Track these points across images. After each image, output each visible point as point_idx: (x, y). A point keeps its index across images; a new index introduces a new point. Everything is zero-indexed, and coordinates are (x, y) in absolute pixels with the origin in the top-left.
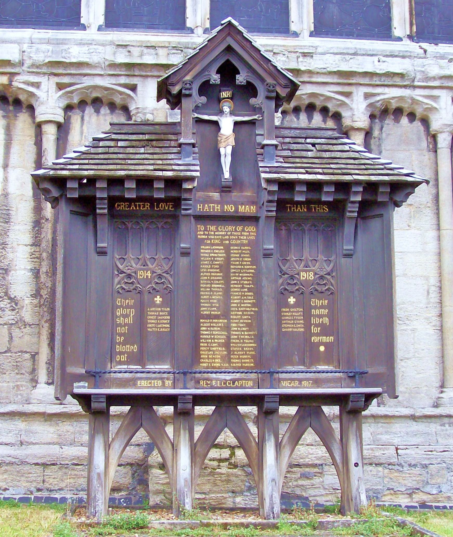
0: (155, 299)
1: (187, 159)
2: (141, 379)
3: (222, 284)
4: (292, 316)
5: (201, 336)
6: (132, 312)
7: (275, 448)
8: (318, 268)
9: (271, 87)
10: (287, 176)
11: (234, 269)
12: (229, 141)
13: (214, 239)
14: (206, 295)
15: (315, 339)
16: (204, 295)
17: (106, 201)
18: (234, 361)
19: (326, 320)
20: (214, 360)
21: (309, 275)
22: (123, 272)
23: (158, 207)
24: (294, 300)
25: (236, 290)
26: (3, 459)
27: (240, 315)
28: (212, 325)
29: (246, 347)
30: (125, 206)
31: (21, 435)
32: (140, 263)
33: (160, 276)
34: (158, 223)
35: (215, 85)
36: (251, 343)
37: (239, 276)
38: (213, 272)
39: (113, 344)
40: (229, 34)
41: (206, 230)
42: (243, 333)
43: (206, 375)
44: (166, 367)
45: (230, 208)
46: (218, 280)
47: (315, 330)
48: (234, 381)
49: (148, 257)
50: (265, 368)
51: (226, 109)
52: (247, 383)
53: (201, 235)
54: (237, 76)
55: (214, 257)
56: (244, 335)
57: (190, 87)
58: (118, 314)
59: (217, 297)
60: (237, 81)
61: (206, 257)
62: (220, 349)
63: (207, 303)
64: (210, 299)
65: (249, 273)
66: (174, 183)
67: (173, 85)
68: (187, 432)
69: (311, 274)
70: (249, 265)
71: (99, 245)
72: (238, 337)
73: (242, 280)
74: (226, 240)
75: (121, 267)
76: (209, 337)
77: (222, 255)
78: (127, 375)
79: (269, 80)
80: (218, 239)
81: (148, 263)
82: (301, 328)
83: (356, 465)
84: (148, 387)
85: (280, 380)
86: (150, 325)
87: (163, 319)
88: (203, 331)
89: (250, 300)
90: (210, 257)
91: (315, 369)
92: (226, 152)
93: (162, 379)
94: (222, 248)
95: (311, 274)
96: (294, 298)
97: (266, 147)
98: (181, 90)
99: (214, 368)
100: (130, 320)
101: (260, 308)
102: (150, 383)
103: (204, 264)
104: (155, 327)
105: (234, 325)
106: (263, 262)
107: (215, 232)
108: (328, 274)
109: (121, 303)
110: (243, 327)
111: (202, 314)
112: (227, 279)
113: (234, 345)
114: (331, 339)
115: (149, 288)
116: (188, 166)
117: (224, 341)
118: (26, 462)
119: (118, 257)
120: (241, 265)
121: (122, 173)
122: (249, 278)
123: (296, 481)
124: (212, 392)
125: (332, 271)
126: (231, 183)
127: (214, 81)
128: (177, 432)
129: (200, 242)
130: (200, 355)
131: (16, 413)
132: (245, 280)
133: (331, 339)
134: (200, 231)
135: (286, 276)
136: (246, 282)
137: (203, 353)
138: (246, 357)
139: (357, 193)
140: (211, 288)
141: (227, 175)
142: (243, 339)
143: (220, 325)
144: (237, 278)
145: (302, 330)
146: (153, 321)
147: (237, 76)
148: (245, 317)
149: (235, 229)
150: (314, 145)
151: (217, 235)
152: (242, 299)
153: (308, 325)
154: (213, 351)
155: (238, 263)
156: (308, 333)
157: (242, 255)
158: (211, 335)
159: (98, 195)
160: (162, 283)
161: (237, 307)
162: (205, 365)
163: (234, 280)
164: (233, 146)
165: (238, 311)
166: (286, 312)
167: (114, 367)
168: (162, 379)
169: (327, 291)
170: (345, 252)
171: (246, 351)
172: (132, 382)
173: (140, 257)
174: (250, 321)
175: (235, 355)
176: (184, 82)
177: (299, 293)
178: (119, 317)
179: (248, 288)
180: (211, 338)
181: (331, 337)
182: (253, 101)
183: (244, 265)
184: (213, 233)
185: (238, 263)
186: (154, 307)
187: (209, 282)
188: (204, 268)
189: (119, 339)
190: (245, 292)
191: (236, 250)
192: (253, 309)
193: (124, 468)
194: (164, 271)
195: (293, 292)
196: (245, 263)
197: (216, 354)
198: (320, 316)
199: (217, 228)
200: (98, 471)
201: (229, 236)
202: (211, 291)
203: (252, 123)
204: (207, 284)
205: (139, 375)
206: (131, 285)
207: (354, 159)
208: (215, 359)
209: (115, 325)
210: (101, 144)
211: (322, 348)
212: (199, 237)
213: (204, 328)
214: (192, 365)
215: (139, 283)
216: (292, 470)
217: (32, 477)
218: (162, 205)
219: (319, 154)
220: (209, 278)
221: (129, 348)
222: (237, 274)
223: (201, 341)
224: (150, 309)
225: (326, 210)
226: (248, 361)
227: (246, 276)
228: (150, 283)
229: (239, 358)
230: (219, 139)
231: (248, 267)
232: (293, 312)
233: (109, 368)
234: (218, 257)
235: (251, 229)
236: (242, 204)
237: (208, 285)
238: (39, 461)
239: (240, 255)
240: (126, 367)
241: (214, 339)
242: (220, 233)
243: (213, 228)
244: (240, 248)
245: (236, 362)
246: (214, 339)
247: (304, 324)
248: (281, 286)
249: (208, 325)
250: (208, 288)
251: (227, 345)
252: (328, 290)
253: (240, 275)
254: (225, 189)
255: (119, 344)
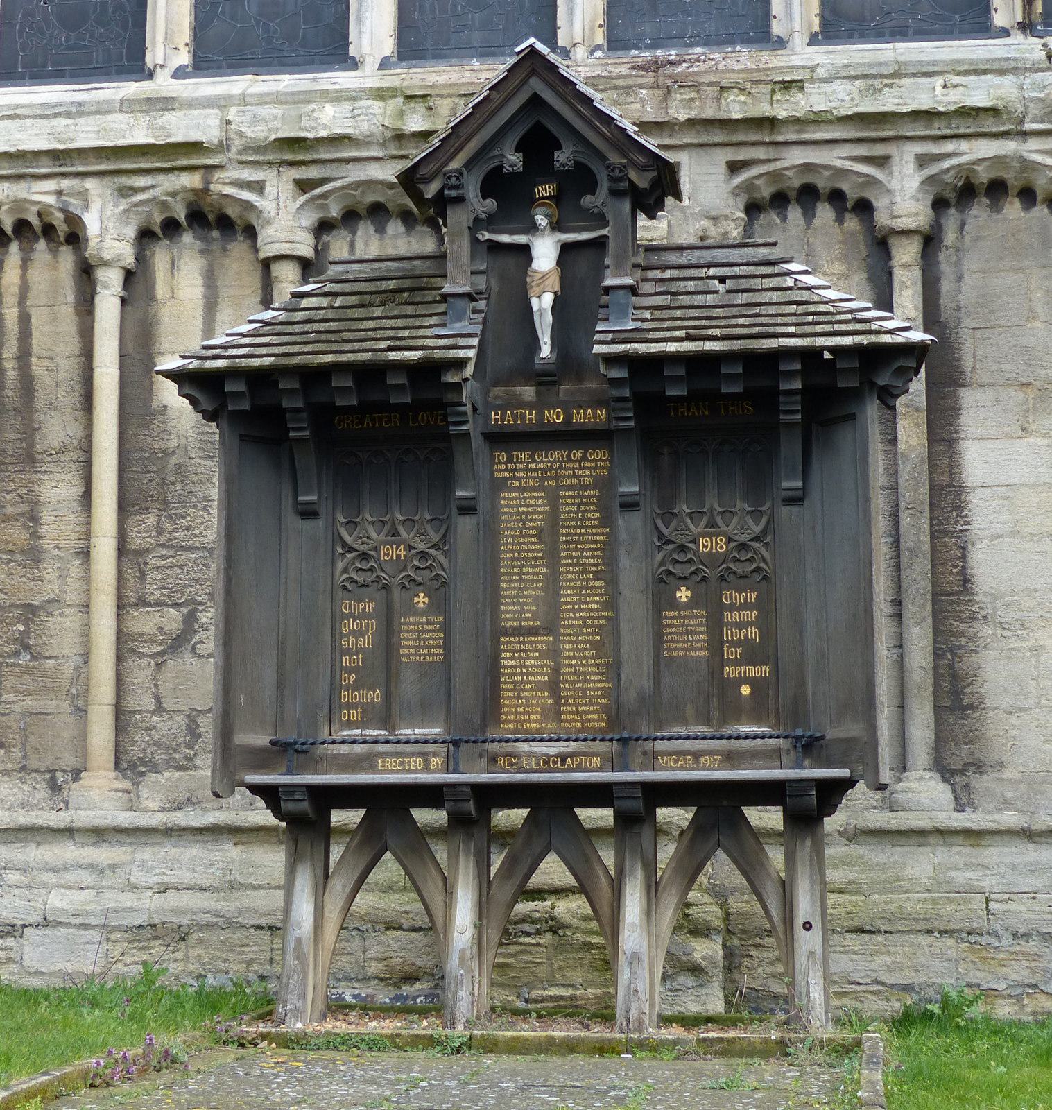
0: (416, 600)
1: (457, 325)
2: (384, 755)
3: (542, 565)
4: (684, 625)
5: (502, 670)
6: (372, 626)
7: (644, 892)
8: (736, 528)
9: (617, 170)
10: (641, 348)
11: (567, 535)
12: (547, 283)
13: (527, 478)
14: (510, 589)
15: (730, 672)
16: (508, 589)
17: (304, 415)
18: (567, 717)
19: (754, 633)
20: (527, 717)
21: (717, 544)
22: (351, 550)
23: (415, 420)
24: (689, 593)
25: (570, 576)
26: (194, 917)
27: (579, 626)
28: (523, 647)
29: (590, 689)
30: (352, 421)
31: (231, 870)
32: (385, 531)
33: (423, 555)
34: (360, 454)
35: (513, 175)
36: (601, 681)
37: (576, 549)
38: (524, 543)
39: (334, 689)
40: (533, 73)
41: (510, 460)
42: (584, 662)
43: (509, 747)
44: (434, 731)
45: (555, 417)
46: (536, 559)
47: (730, 653)
48: (563, 758)
49: (400, 518)
50: (623, 730)
51: (542, 221)
52: (590, 760)
53: (500, 471)
54: (557, 153)
55: (527, 513)
56: (587, 665)
57: (457, 183)
58: (345, 630)
59: (534, 591)
60: (557, 164)
61: (512, 514)
62: (539, 693)
63: (514, 604)
64: (518, 596)
65: (596, 542)
66: (429, 372)
67: (427, 180)
68: (472, 858)
69: (721, 540)
70: (595, 527)
71: (301, 499)
72: (575, 670)
73: (582, 556)
74: (551, 478)
75: (348, 539)
76: (519, 670)
77: (543, 509)
78: (358, 748)
79: (614, 158)
80: (534, 478)
81: (401, 530)
82: (701, 649)
83: (808, 926)
84: (398, 772)
85: (655, 755)
86: (406, 651)
87: (430, 638)
88: (506, 659)
89: (595, 599)
90: (518, 513)
91: (730, 732)
92: (542, 303)
93: (425, 755)
94: (543, 494)
95: (721, 541)
96: (688, 589)
97: (611, 292)
98: (441, 191)
99: (528, 731)
100: (367, 642)
101: (617, 611)
102: (402, 763)
103: (507, 529)
104: (416, 655)
105: (566, 646)
106: (622, 520)
107: (528, 463)
108: (757, 539)
109: (350, 607)
110: (586, 650)
111: (503, 627)
112: (552, 556)
113: (567, 685)
114: (762, 671)
115: (402, 578)
116: (457, 338)
117: (546, 678)
118: (238, 923)
119: (343, 520)
120: (581, 527)
121: (328, 358)
122: (596, 553)
123: (772, 964)
124: (507, 780)
125: (764, 532)
126: (554, 366)
127: (510, 166)
128: (454, 858)
129: (498, 485)
130: (500, 707)
131: (223, 828)
132: (587, 557)
133: (762, 671)
134: (500, 462)
135: (671, 546)
136: (591, 561)
137: (506, 702)
138: (591, 708)
139: (790, 375)
140: (520, 574)
141: (546, 351)
142: (584, 673)
143: (539, 646)
144: (573, 554)
145: (705, 653)
146: (411, 643)
147: (557, 153)
148: (589, 630)
149: (568, 456)
150: (722, 280)
151: (532, 470)
152: (583, 595)
153: (716, 644)
154: (527, 699)
155: (573, 523)
156: (717, 659)
157: (582, 508)
158: (521, 666)
159: (286, 404)
160: (427, 567)
161: (574, 611)
162: (511, 726)
163: (566, 558)
164: (555, 293)
165: (575, 618)
166: (671, 618)
167: (336, 732)
168: (425, 755)
169: (755, 574)
170: (784, 494)
171: (591, 697)
172: (367, 762)
173: (385, 519)
174: (598, 638)
175: (570, 705)
176: (445, 175)
177: (698, 581)
178: (347, 636)
179: (595, 573)
180: (522, 674)
181: (764, 668)
182: (587, 201)
183: (586, 527)
184: (524, 466)
185: (573, 523)
186: (414, 615)
187: (517, 563)
188: (507, 536)
189: (347, 679)
190: (588, 580)
191: (569, 497)
192: (605, 614)
193: (426, 935)
194: (430, 545)
195: (685, 578)
196: (588, 523)
197: (532, 705)
198: (740, 625)
199: (532, 456)
200: (298, 933)
201: (556, 470)
202: (521, 580)
203: (599, 245)
204: (513, 567)
205: (380, 748)
206: (369, 573)
207: (799, 303)
208: (529, 714)
209: (336, 650)
210: (305, 303)
211: (745, 690)
212: (496, 474)
213: (507, 655)
214: (484, 726)
215: (382, 570)
216: (762, 942)
217: (249, 953)
218: (423, 416)
219: (728, 299)
220: (516, 554)
221: (364, 696)
222: (573, 546)
223: (502, 679)
224: (405, 619)
225: (749, 410)
226: (595, 716)
227: (591, 550)
228: (405, 569)
229: (577, 712)
230: (528, 280)
231: (594, 530)
232: (685, 618)
233: (324, 734)
234: (535, 513)
235: (598, 455)
236: (580, 407)
237: (515, 570)
238: (262, 922)
239: (578, 508)
240: (358, 731)
241: (527, 674)
242: (539, 466)
243: (524, 456)
244: (579, 493)
245: (571, 720)
246: (527, 674)
247: (707, 641)
248: (660, 566)
249: (516, 647)
250: (515, 574)
251: (554, 686)
252: (758, 570)
253: (579, 546)
254: (545, 379)
255: (347, 688)
